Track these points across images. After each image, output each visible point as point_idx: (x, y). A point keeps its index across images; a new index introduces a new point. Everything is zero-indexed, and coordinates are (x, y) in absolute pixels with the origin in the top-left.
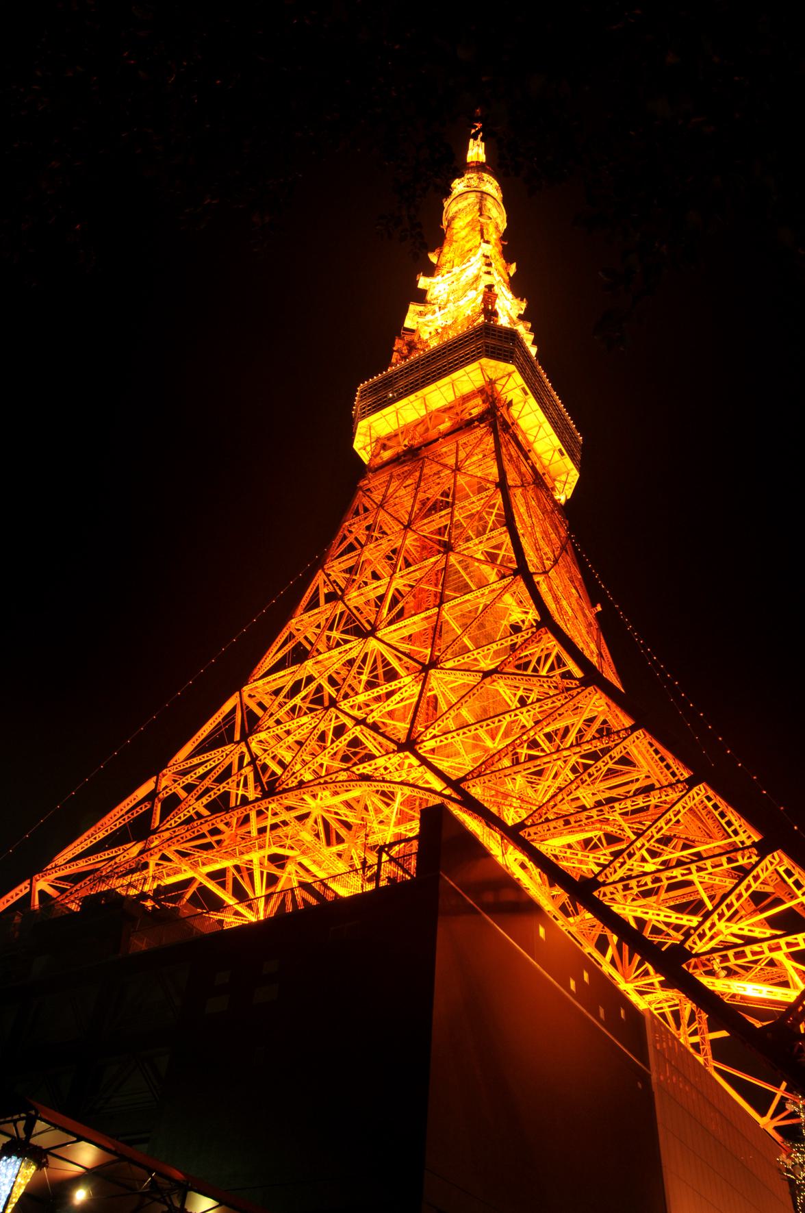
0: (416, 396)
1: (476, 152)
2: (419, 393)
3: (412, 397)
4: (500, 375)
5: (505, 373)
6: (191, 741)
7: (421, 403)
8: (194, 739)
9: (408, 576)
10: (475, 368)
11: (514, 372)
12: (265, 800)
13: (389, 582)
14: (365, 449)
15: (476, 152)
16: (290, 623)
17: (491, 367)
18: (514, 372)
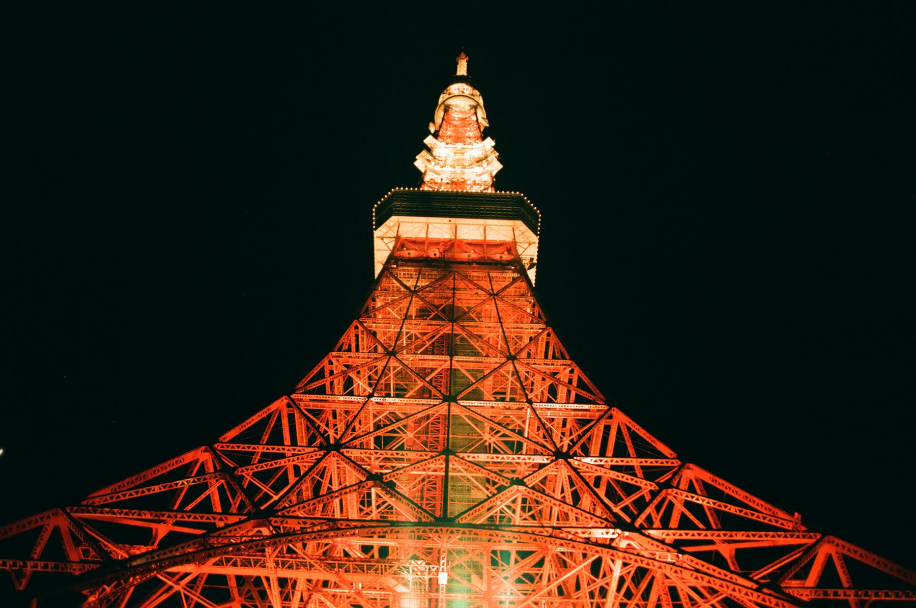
0: (450, 221)
1: (462, 69)
2: (453, 220)
3: (446, 220)
4: (522, 240)
5: (527, 241)
6: (239, 427)
7: (451, 228)
8: (243, 424)
9: (462, 363)
10: (507, 224)
11: (534, 243)
12: (448, 528)
13: (504, 363)
14: (382, 239)
15: (462, 69)
16: (330, 354)
17: (520, 230)
18: (534, 243)
